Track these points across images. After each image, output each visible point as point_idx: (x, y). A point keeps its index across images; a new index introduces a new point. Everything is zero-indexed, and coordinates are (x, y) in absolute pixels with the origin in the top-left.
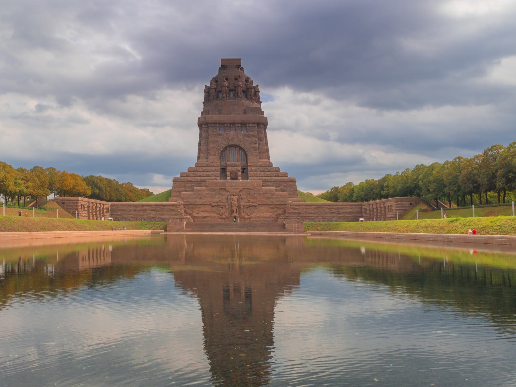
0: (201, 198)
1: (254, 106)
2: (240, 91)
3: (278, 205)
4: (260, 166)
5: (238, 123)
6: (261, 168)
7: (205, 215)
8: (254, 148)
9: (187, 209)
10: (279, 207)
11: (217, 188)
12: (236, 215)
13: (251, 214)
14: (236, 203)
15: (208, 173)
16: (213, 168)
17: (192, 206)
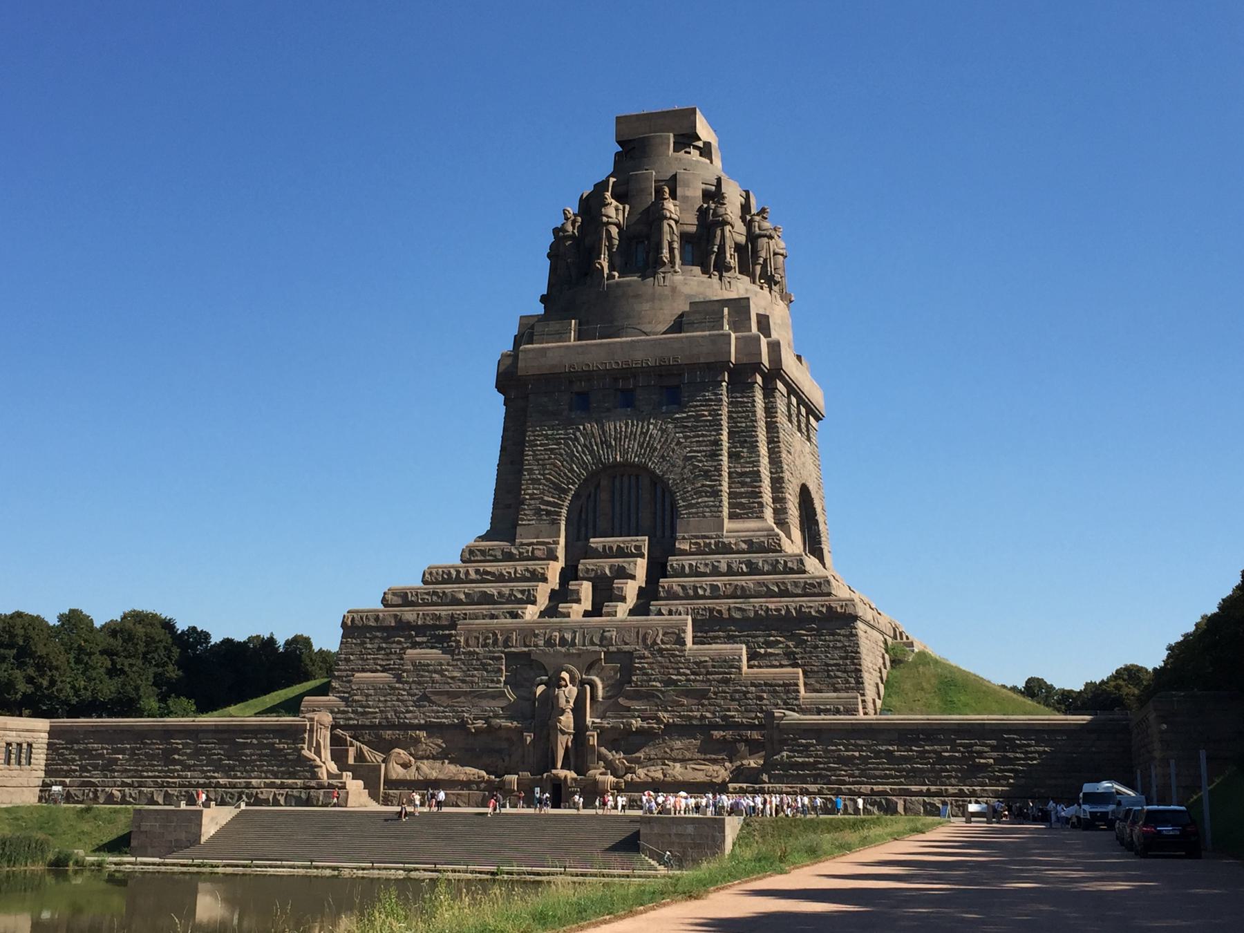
0: (425, 697)
1: (733, 295)
2: (667, 237)
3: (752, 727)
4: (726, 549)
5: (647, 371)
6: (723, 561)
7: (434, 775)
8: (706, 474)
9: (365, 748)
10: (756, 735)
11: (498, 651)
12: (562, 773)
13: (629, 770)
14: (567, 720)
15: (492, 589)
16: (520, 567)
17: (388, 734)
